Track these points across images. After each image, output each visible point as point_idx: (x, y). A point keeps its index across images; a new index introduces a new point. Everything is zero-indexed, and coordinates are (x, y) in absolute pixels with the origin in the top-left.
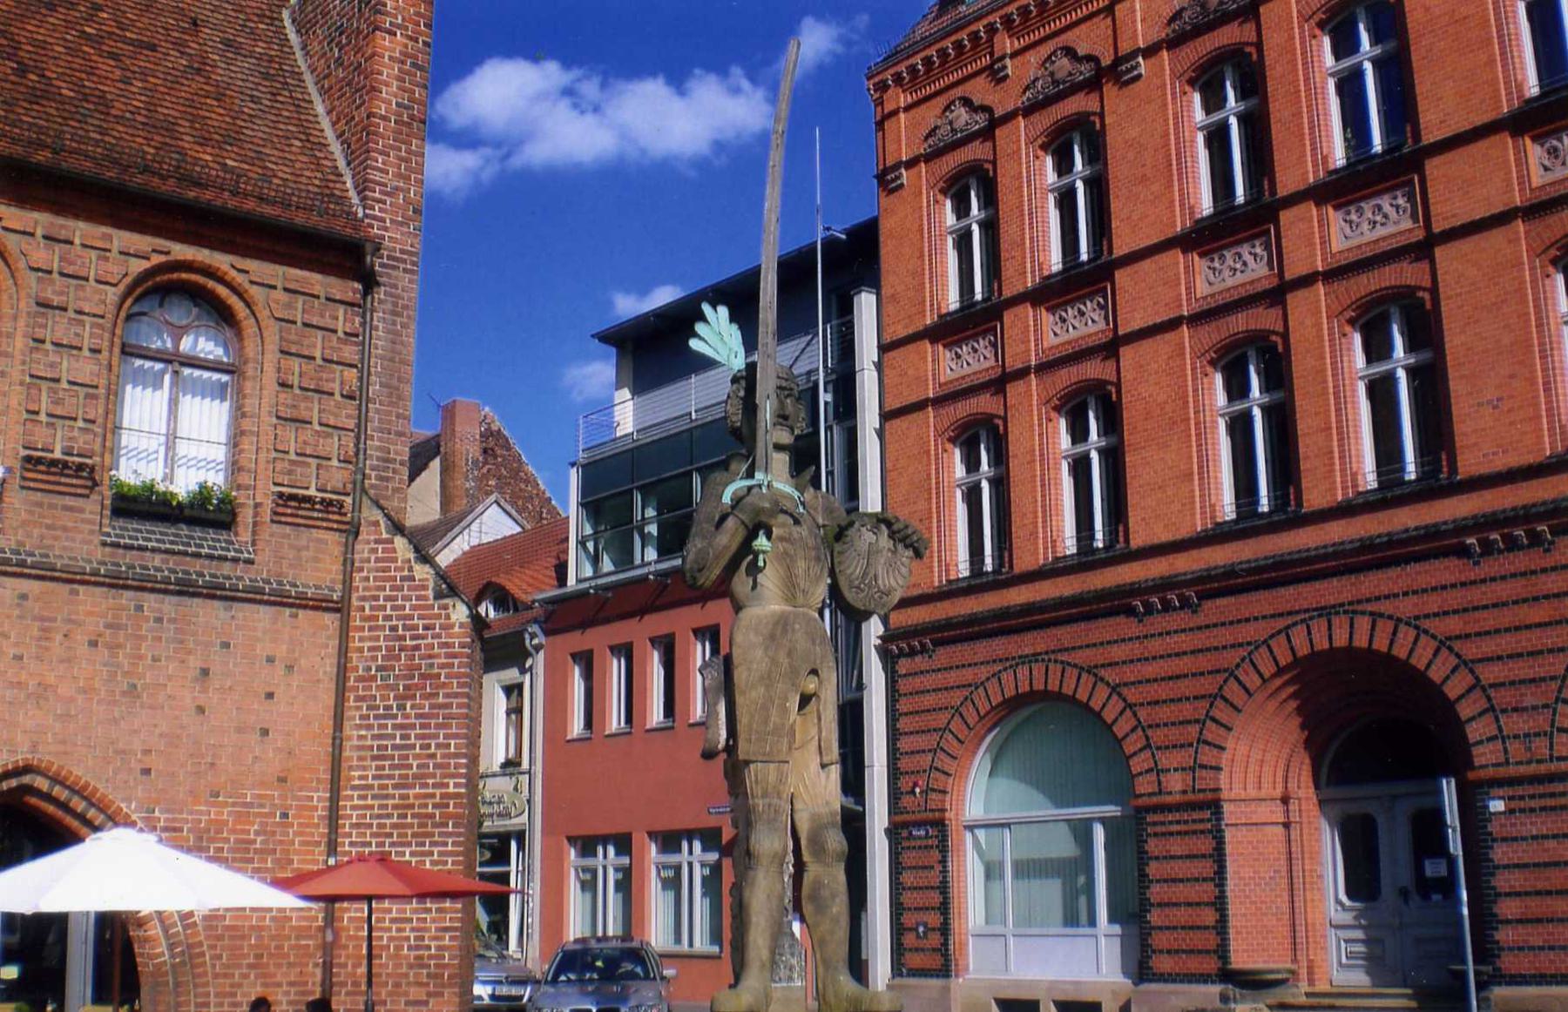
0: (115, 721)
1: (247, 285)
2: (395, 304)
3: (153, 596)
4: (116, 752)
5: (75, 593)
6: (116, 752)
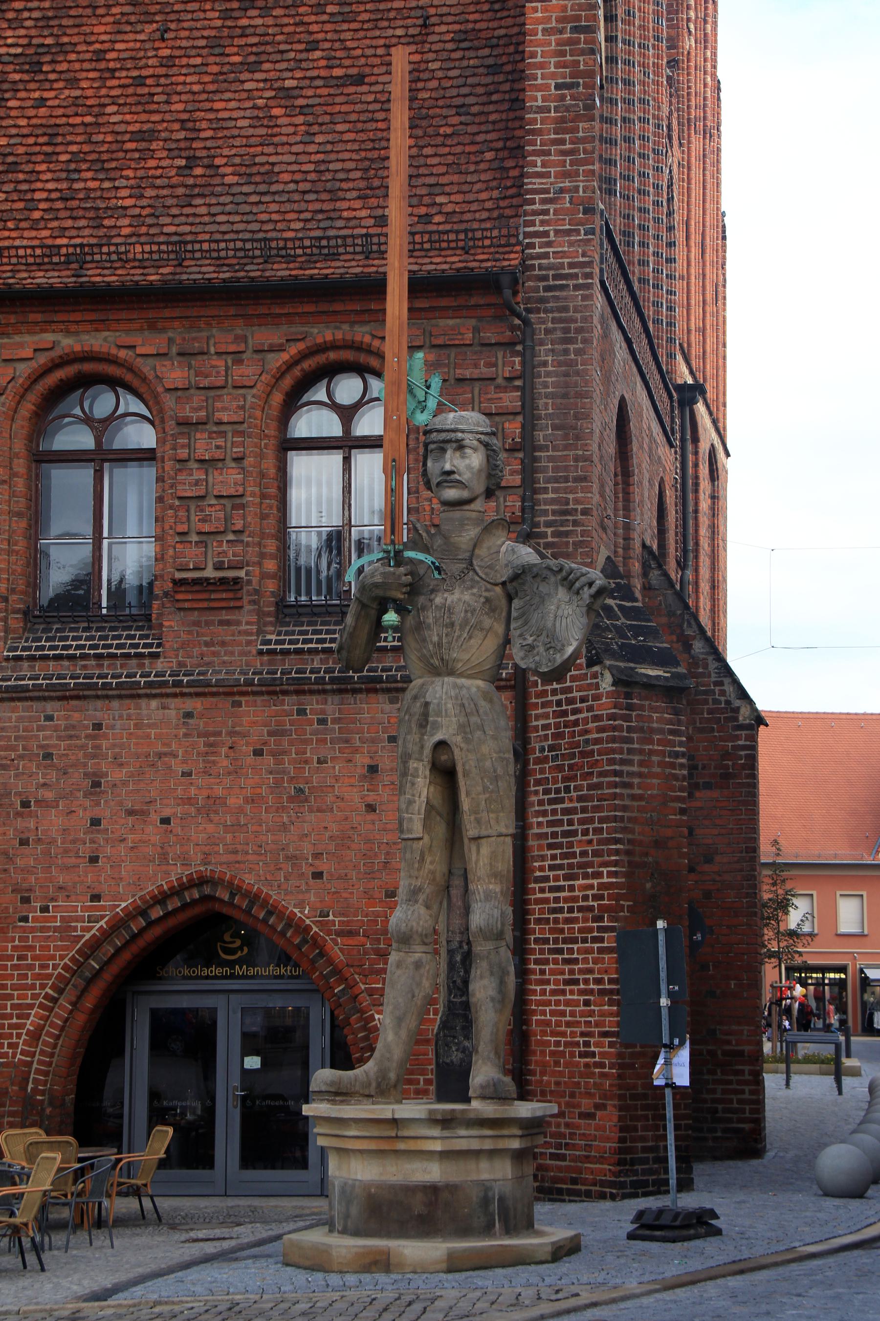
0: (284, 828)
2: (567, 330)
4: (287, 858)
6: (287, 858)
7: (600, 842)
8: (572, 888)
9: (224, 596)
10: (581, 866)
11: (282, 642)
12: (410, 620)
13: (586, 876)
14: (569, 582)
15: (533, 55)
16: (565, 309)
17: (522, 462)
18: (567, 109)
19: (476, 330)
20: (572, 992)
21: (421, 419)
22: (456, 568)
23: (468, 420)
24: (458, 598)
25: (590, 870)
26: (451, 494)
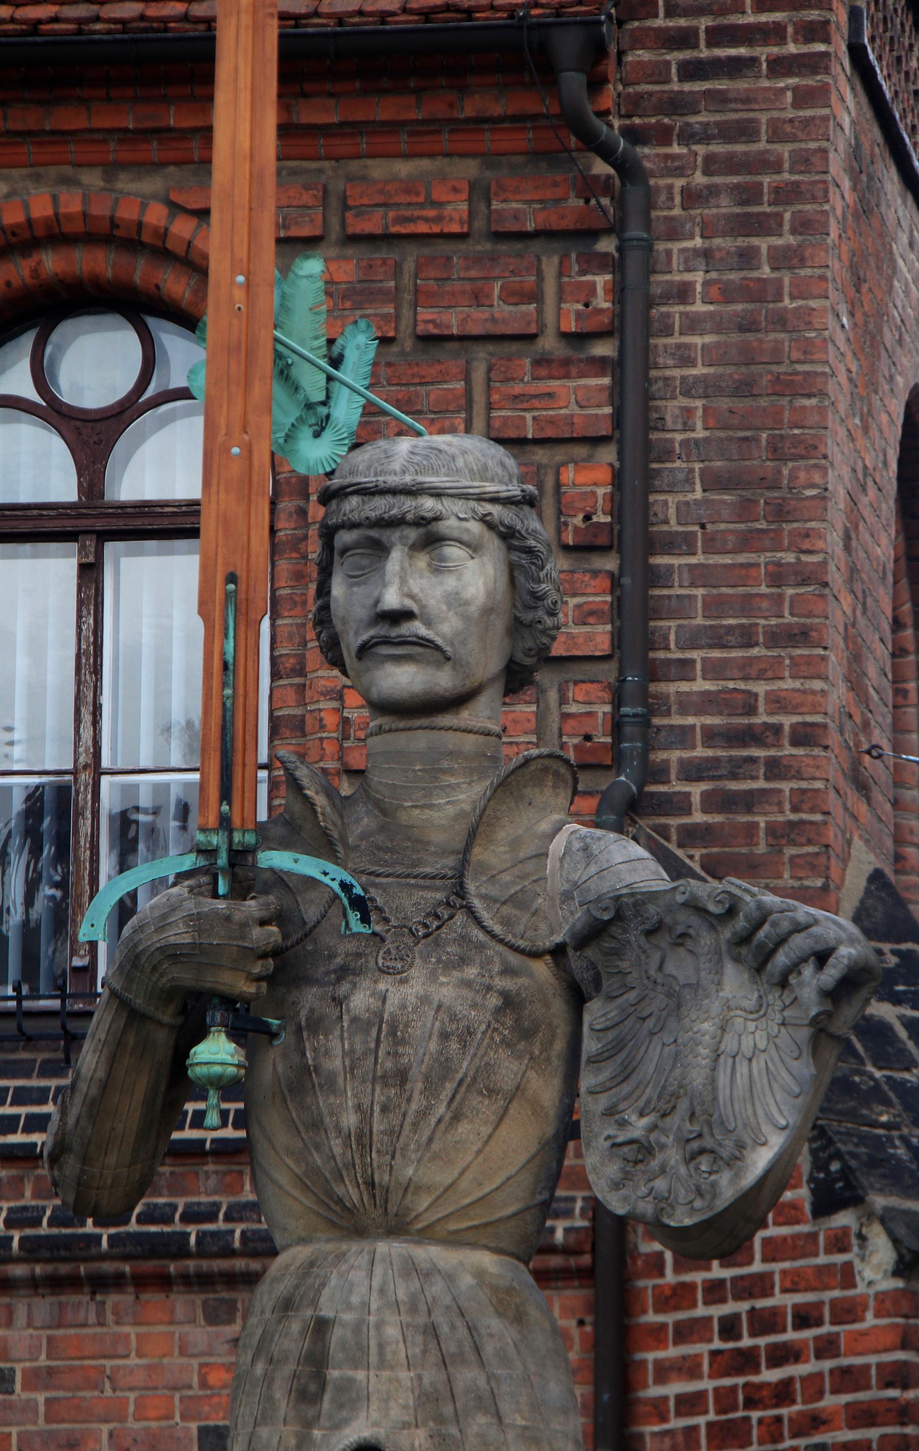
12: (275, 1063)
14: (756, 949)
16: (744, 131)
17: (615, 582)
19: (480, 192)
21: (315, 454)
22: (410, 903)
23: (452, 460)
24: (420, 995)
26: (402, 678)
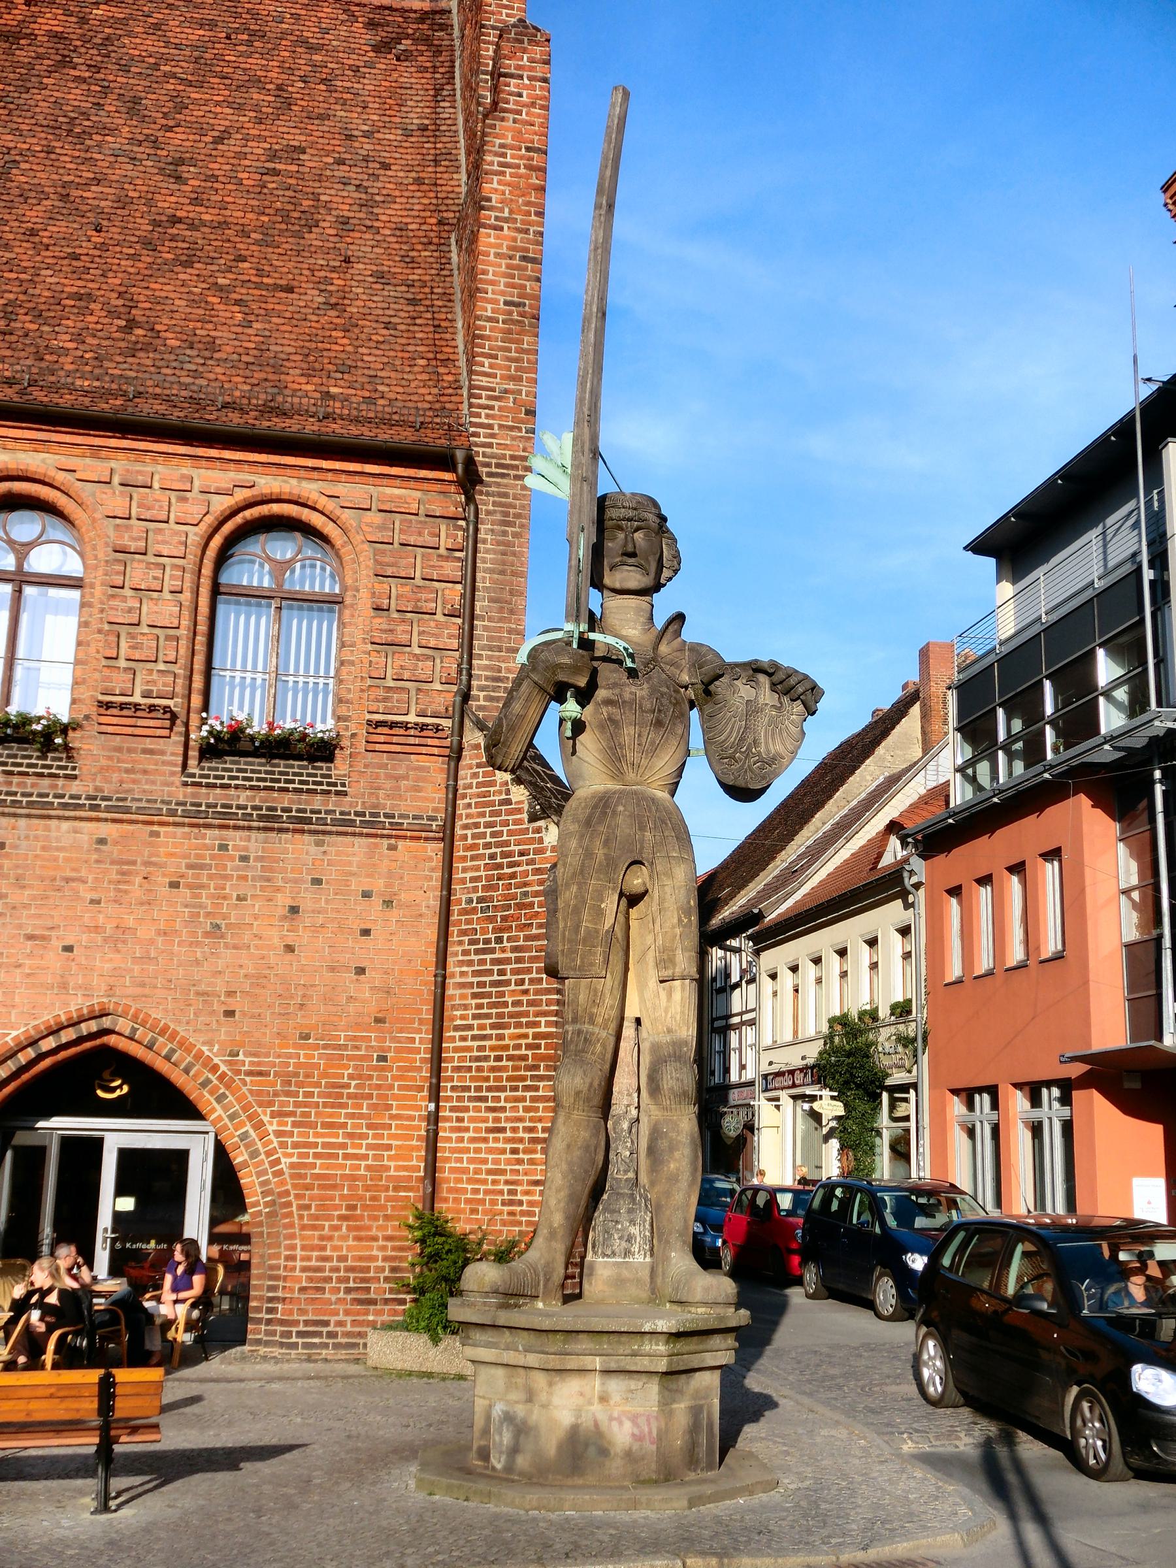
0: (197, 962)
1: (338, 512)
2: (507, 514)
3: (239, 834)
5: (156, 834)
6: (198, 994)
7: (537, 992)
8: (501, 1037)
9: (151, 723)
10: (511, 1015)
11: (208, 777)
13: (519, 1025)
15: (485, 272)
16: (506, 495)
18: (513, 322)
20: (496, 1140)
25: (524, 1020)
